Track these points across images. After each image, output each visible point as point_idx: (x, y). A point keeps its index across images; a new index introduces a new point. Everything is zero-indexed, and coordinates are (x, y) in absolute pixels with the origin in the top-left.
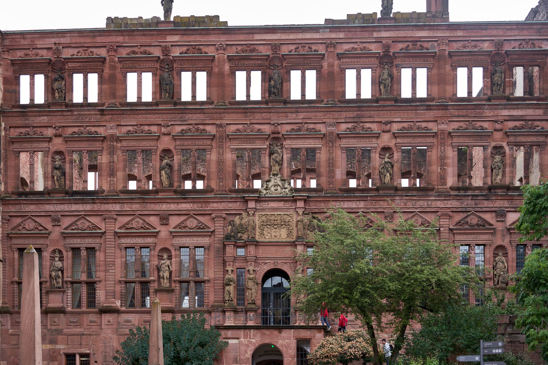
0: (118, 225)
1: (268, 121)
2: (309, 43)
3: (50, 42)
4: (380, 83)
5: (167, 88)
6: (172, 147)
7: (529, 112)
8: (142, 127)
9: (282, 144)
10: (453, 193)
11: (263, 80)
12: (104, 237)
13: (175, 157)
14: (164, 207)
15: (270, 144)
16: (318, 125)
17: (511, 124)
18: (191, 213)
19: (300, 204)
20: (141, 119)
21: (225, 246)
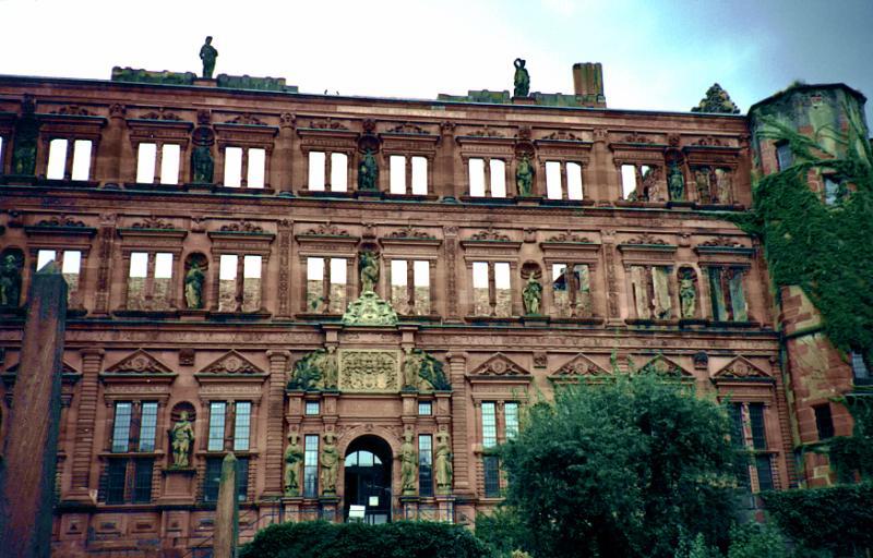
0: (105, 365)
1: (358, 221)
2: (425, 122)
3: (18, 93)
4: (518, 179)
5: (202, 168)
6: (206, 251)
7: (723, 225)
8: (159, 220)
9: (378, 253)
10: (630, 327)
11: (350, 165)
12: (79, 384)
13: (210, 265)
14: (188, 338)
15: (360, 253)
16: (432, 229)
17: (701, 240)
18: (233, 348)
19: (408, 338)
20: (159, 207)
21: (286, 400)
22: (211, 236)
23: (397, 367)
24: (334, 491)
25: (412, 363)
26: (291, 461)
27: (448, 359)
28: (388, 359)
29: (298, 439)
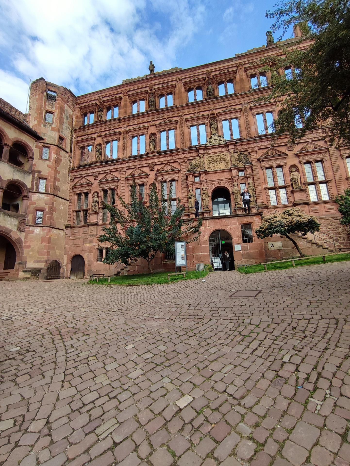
0: (127, 175)
1: (208, 109)
14: (152, 161)
18: (167, 162)
22: (157, 126)
23: (228, 159)
24: (208, 208)
25: (234, 156)
26: (190, 198)
27: (249, 153)
28: (224, 157)
29: (192, 190)
